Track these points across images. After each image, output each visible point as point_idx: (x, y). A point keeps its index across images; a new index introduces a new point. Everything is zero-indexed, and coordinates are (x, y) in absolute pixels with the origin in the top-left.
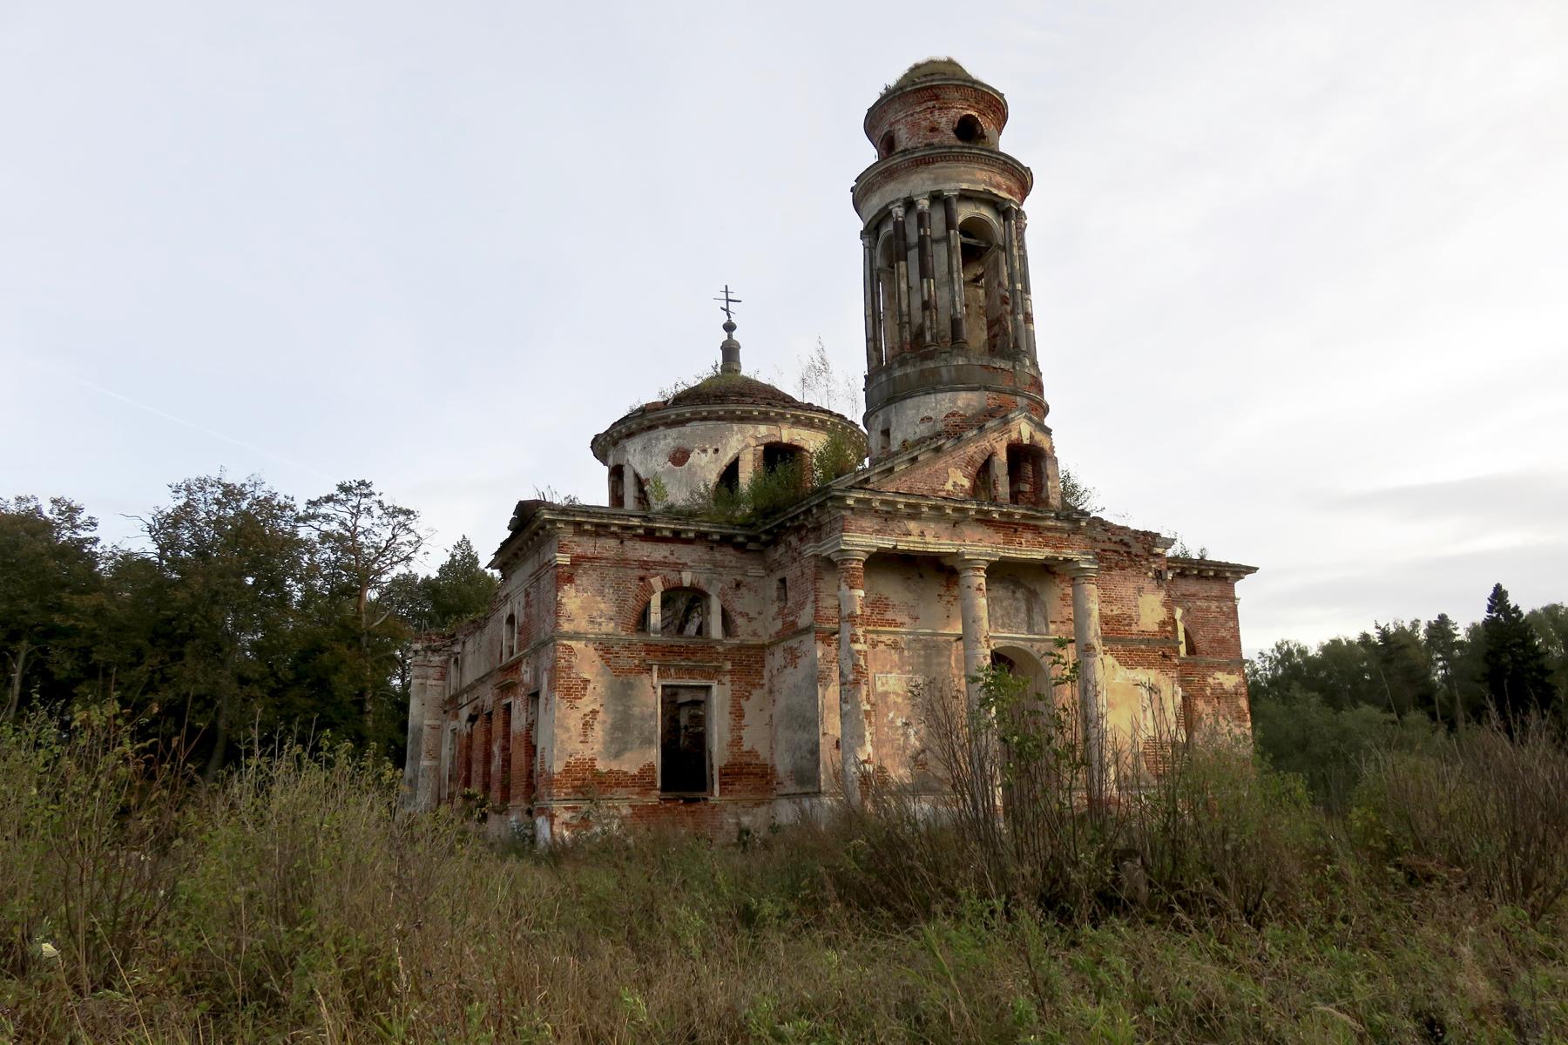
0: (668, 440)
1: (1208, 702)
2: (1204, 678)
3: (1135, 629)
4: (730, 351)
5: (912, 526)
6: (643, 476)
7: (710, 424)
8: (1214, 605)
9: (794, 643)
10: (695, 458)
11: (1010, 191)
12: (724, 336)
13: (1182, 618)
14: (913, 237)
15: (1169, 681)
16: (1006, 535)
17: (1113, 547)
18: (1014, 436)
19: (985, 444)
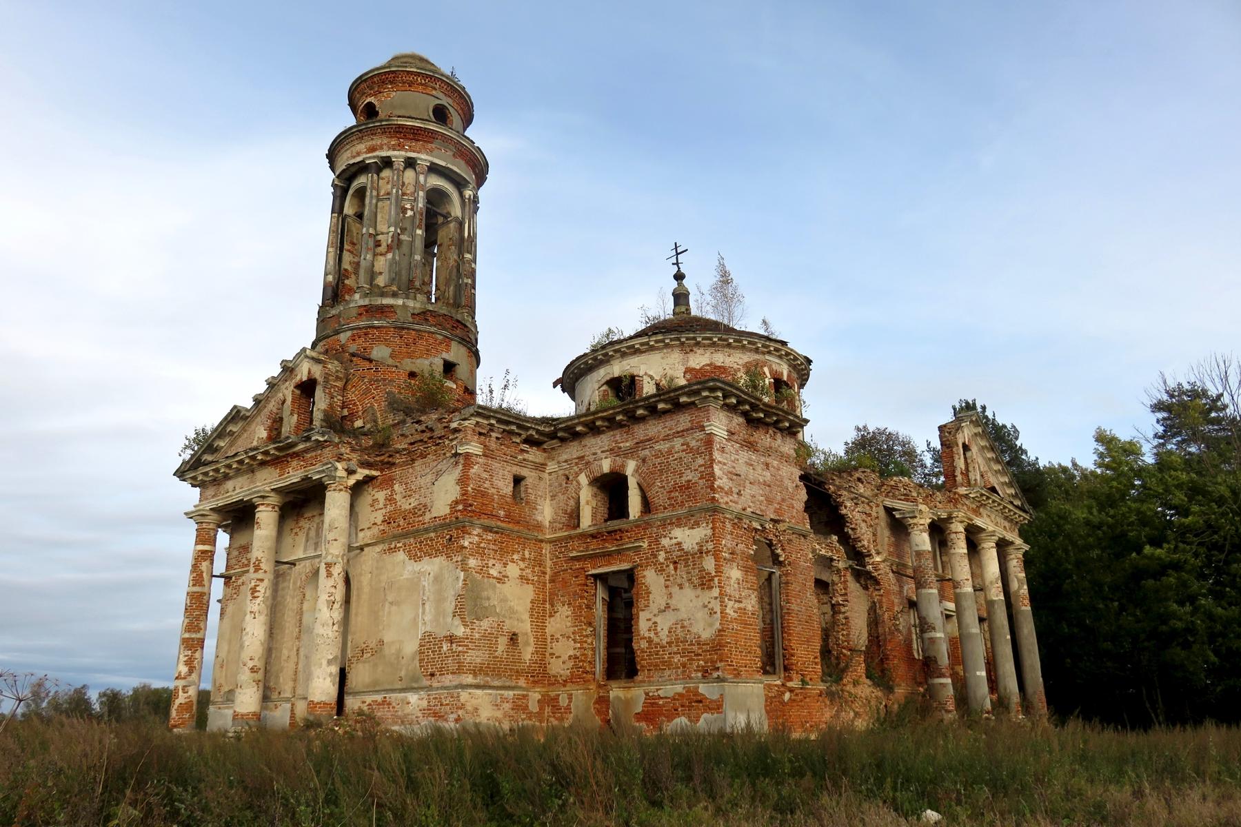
1: (661, 571)
2: (657, 542)
3: (427, 517)
4: (681, 297)
5: (230, 485)
8: (678, 443)
11: (372, 149)
12: (674, 284)
13: (636, 471)
15: (452, 566)
16: (282, 469)
17: (418, 437)
18: (298, 378)
19: (280, 395)
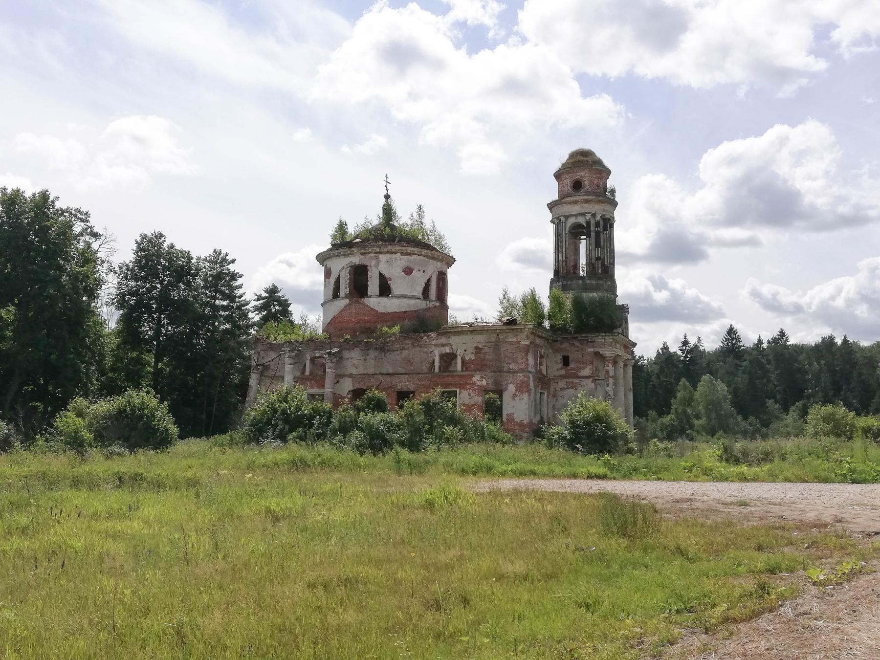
0: (401, 261)
4: (388, 211)
6: (386, 274)
7: (422, 258)
9: (575, 380)
10: (415, 273)
14: (592, 228)
